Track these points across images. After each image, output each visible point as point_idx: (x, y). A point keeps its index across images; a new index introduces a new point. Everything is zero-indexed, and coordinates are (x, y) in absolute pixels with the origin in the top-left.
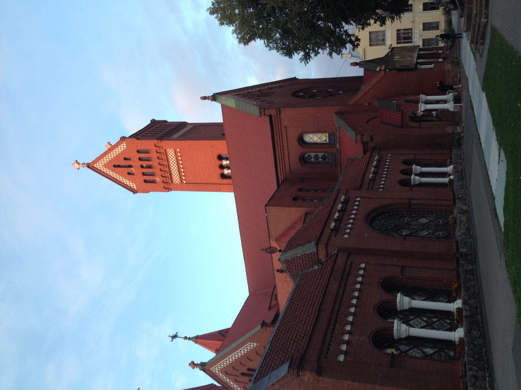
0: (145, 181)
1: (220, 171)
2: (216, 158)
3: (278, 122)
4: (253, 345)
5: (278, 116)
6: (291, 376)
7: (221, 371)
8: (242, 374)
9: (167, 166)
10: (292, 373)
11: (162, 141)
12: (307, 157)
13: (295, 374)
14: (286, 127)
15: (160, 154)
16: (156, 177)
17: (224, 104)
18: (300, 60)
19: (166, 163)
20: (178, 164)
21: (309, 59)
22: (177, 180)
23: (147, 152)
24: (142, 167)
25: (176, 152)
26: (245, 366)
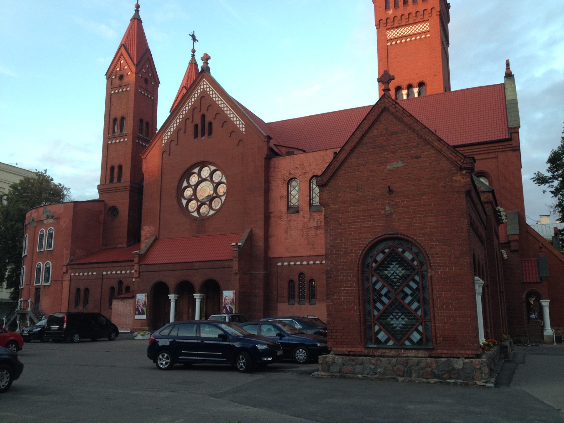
1: (404, 85)
2: (420, 80)
3: (502, 148)
4: (242, 128)
5: (511, 149)
6: (460, 161)
7: (204, 91)
8: (203, 116)
9: (407, 23)
10: (465, 162)
11: (438, 16)
12: (480, 181)
13: (464, 165)
14: (496, 157)
15: (423, 14)
16: (393, 9)
17: (507, 86)
18: (537, 173)
20: (410, 36)
21: (538, 183)
22: (390, 34)
25: (425, 33)
26: (215, 118)
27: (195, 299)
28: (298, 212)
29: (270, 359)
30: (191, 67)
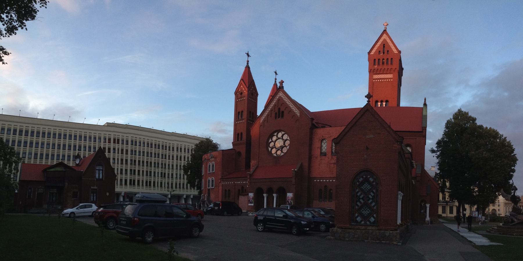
0: (375, 60)
19: (385, 73)
20: (384, 79)
23: (391, 64)
24: (383, 59)
25: (391, 79)
27: (274, 196)
28: (325, 155)
29: (308, 229)
30: (274, 86)
